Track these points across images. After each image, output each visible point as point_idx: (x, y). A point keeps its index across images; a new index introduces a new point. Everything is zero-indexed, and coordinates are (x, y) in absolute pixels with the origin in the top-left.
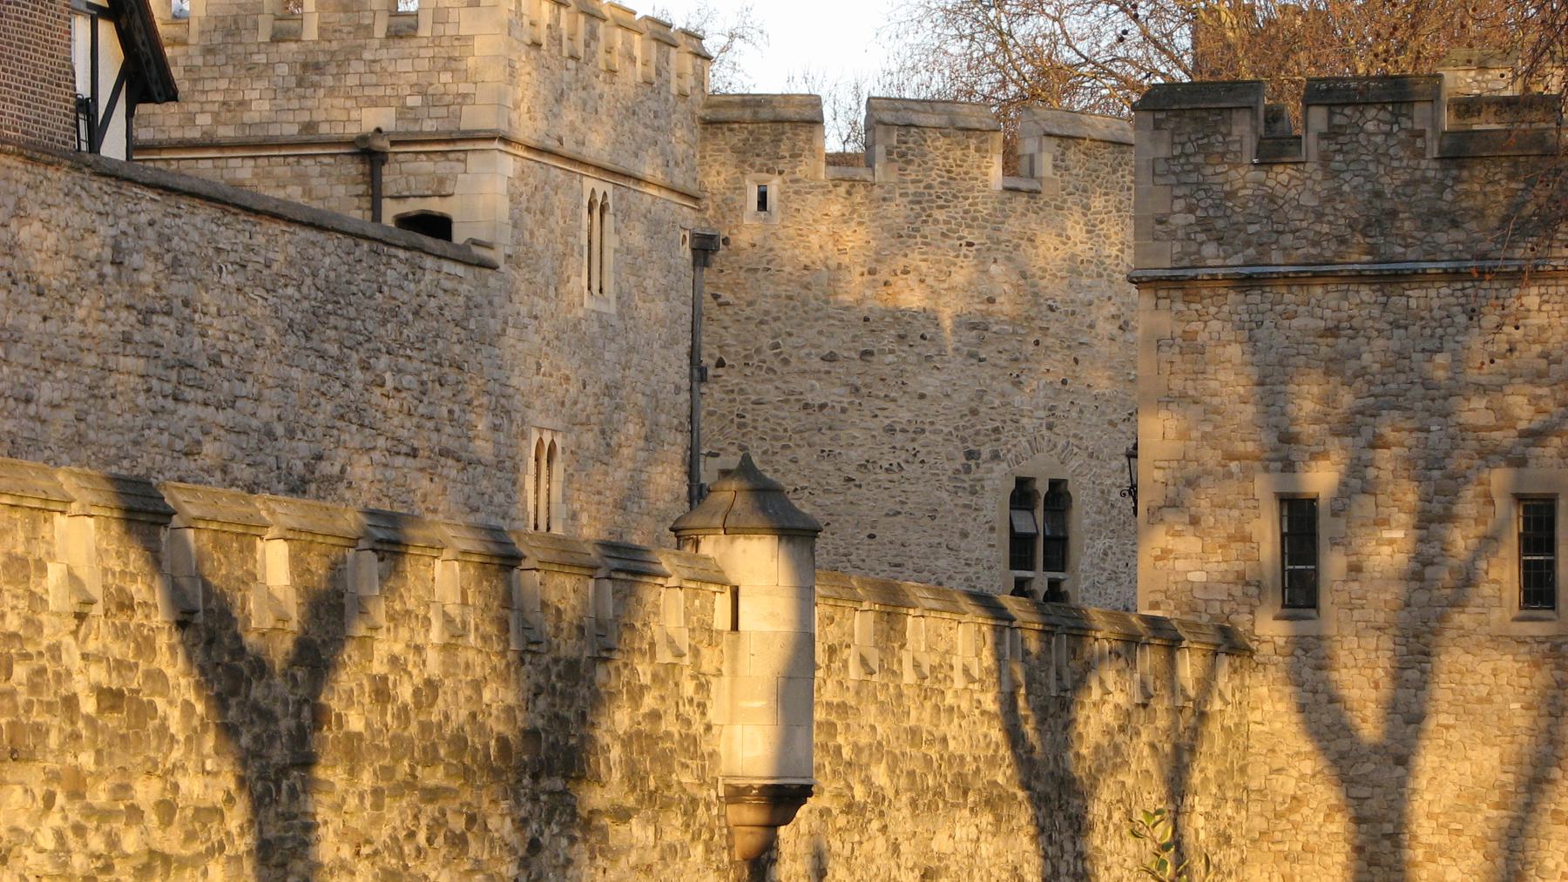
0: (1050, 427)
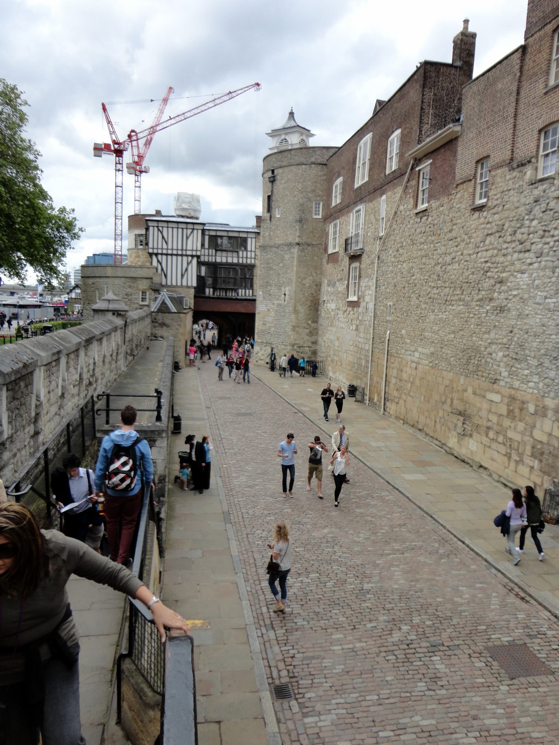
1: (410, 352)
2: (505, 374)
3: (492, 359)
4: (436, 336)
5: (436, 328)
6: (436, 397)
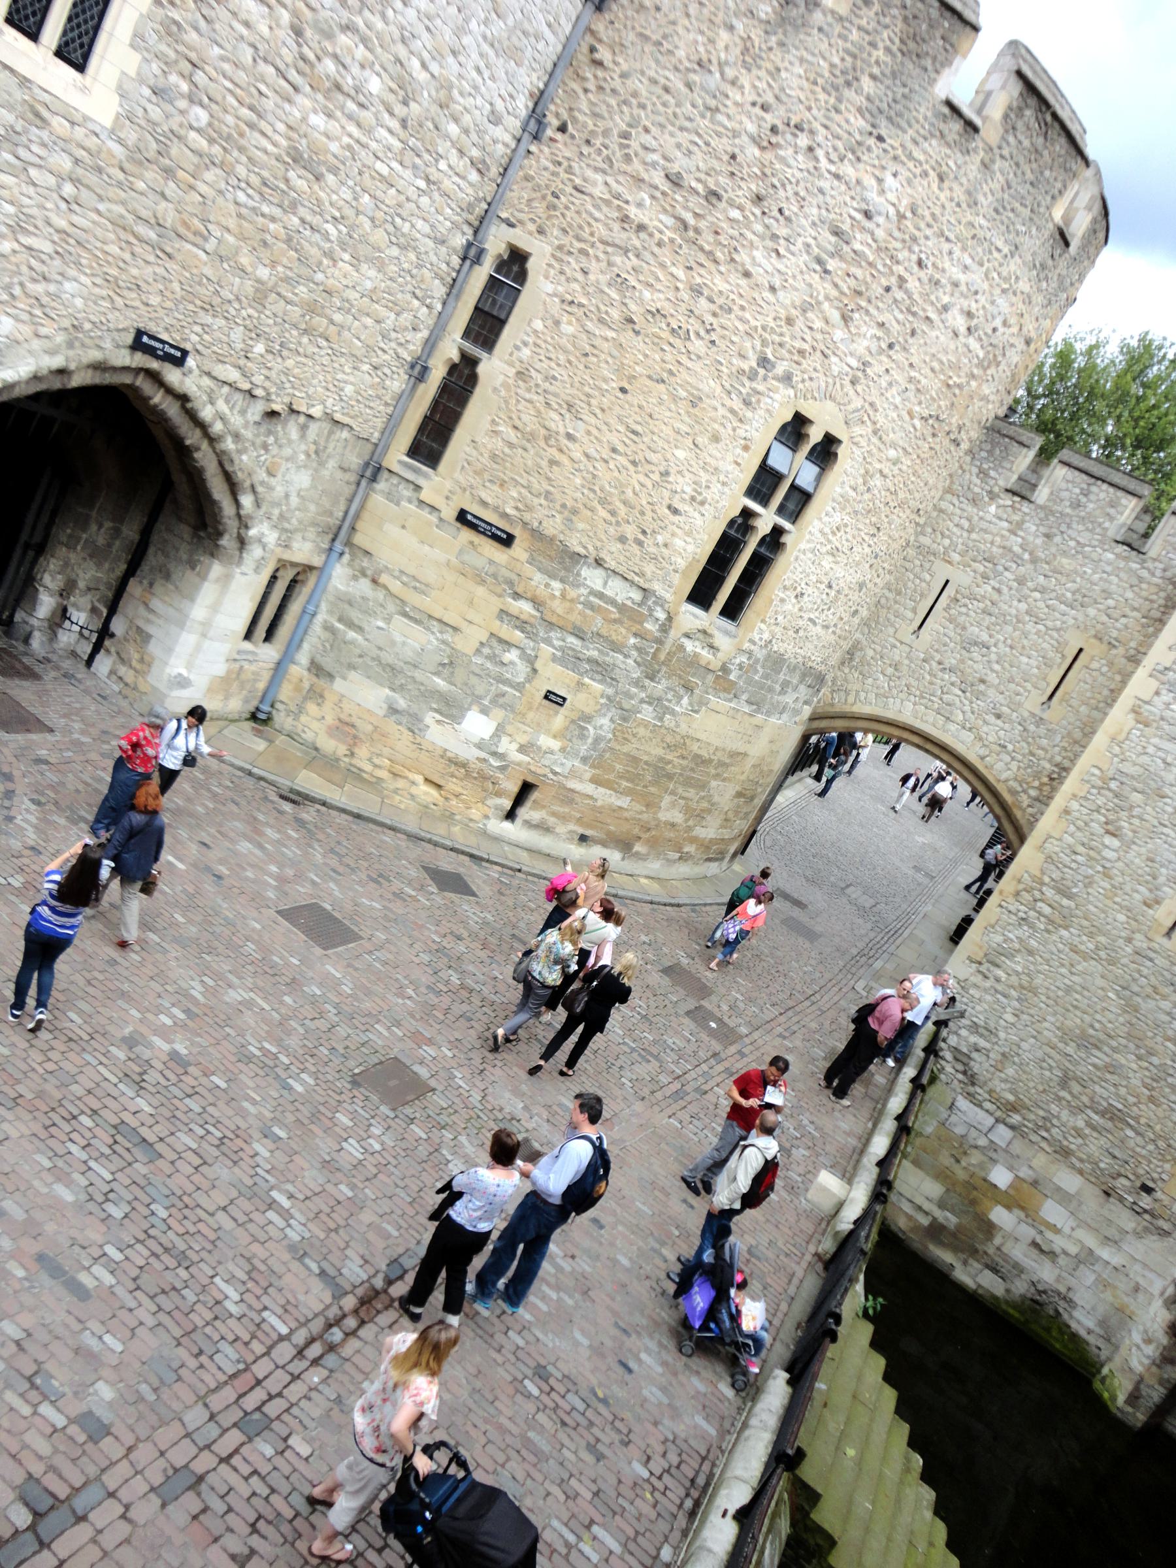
0: (853, 383)
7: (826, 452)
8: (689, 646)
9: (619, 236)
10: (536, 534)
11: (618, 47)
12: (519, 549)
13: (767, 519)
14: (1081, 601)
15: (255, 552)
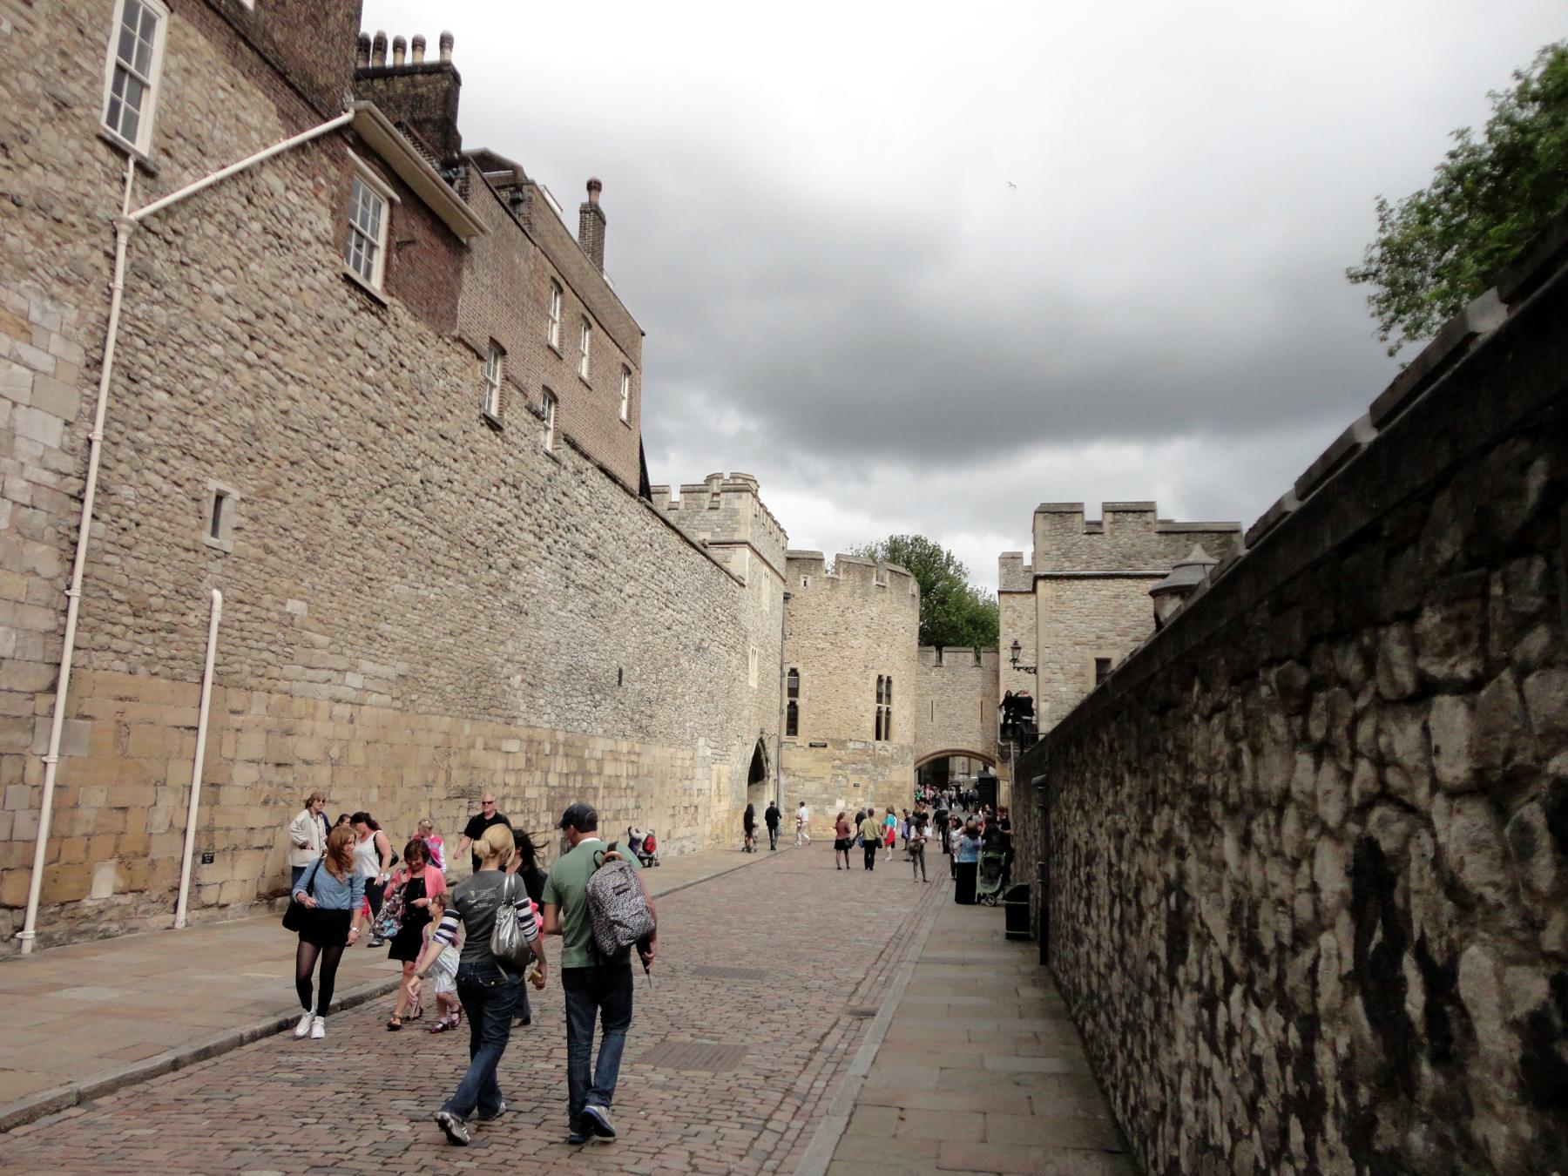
1: (325, 674)
2: (523, 707)
3: (509, 685)
4: (415, 637)
5: (412, 617)
6: (412, 776)
7: (889, 681)
8: (882, 753)
9: (819, 653)
10: (832, 740)
11: (796, 610)
12: (829, 747)
13: (884, 707)
14: (973, 688)
15: (771, 779)
